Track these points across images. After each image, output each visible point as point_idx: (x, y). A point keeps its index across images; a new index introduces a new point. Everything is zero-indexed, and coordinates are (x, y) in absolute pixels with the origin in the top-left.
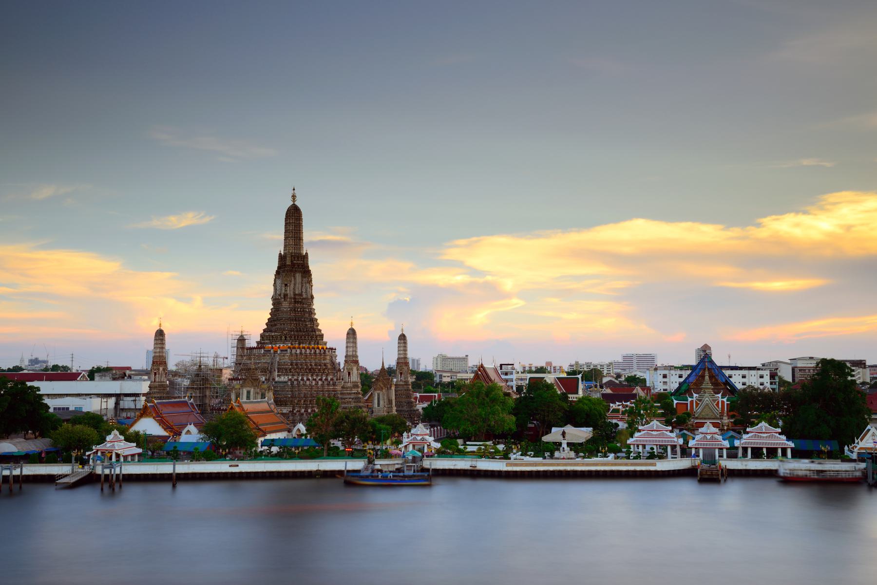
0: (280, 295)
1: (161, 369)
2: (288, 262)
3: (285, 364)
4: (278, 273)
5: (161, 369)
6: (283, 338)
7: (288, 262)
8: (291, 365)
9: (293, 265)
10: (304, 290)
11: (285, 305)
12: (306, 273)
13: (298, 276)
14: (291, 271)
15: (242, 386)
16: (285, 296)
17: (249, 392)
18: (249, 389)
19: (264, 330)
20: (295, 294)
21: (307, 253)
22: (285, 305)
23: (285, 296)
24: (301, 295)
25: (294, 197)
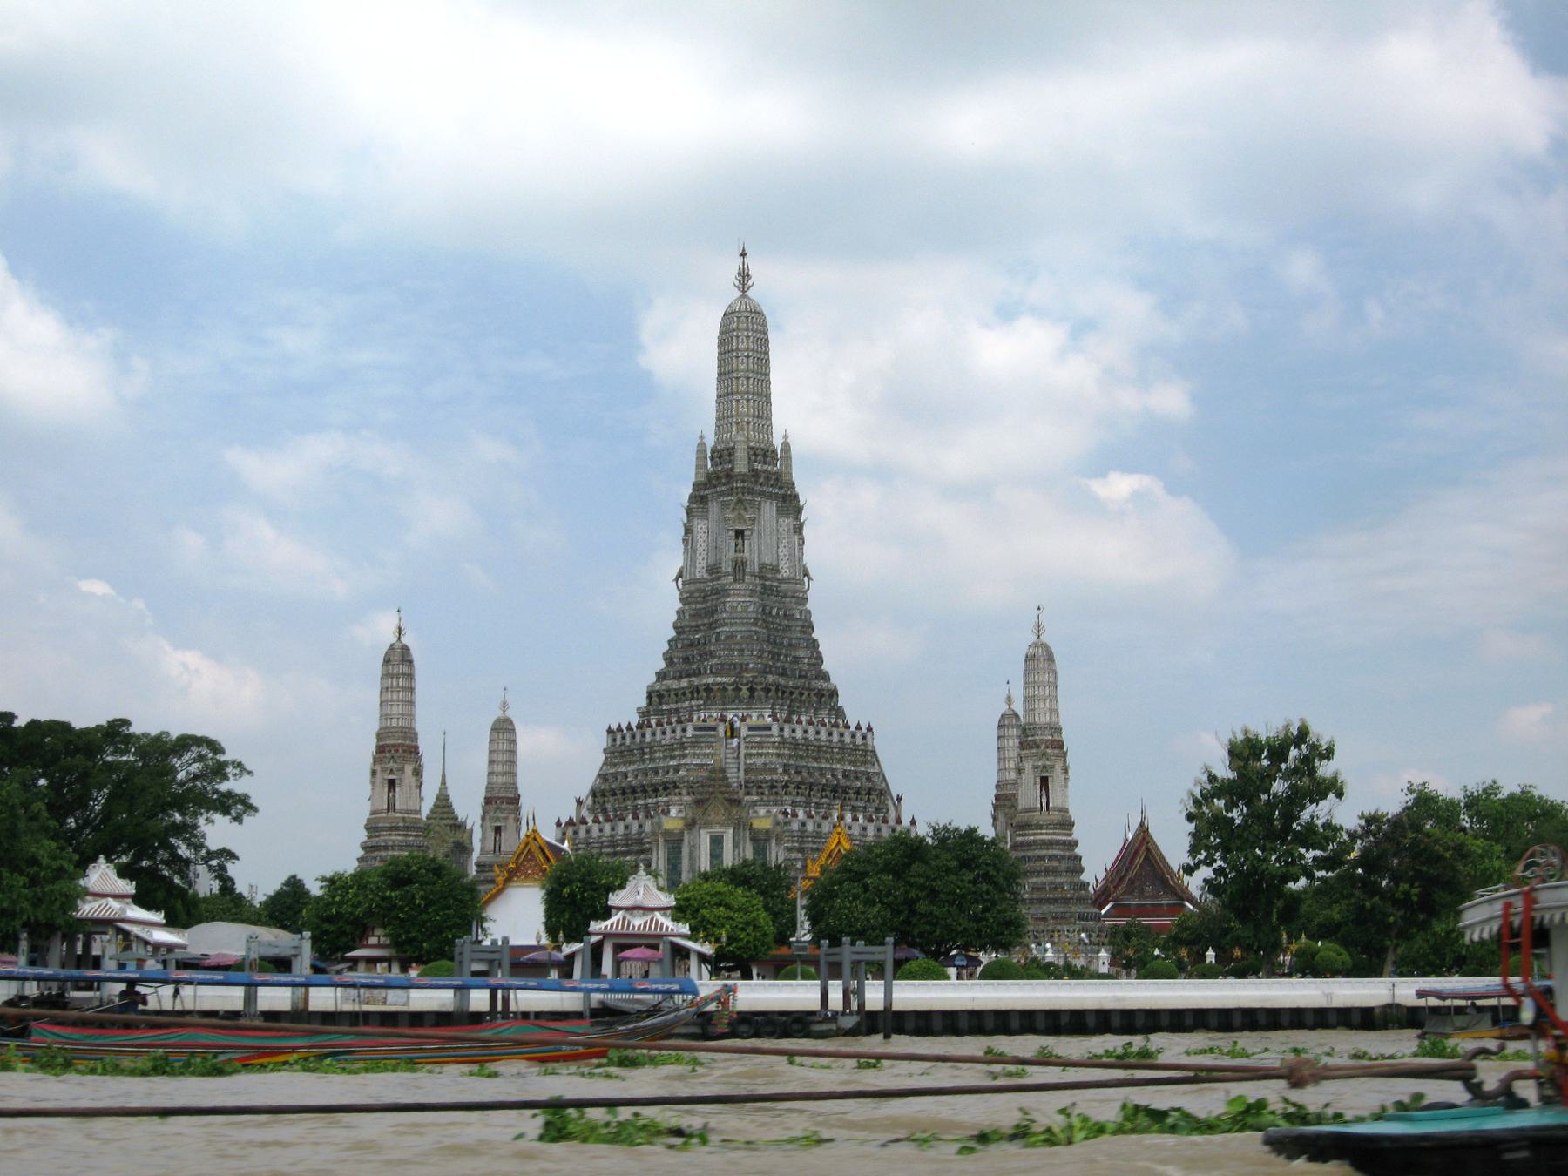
0: (714, 570)
1: (409, 769)
2: (741, 467)
3: (766, 769)
4: (699, 500)
5: (409, 769)
6: (745, 692)
7: (741, 467)
8: (786, 772)
9: (755, 474)
10: (784, 553)
11: (740, 600)
12: (790, 504)
13: (769, 509)
14: (751, 492)
15: (691, 825)
16: (739, 567)
18: (717, 829)
19: (661, 676)
20: (763, 566)
21: (786, 447)
22: (740, 600)
23: (739, 567)
24: (776, 570)
25: (744, 276)
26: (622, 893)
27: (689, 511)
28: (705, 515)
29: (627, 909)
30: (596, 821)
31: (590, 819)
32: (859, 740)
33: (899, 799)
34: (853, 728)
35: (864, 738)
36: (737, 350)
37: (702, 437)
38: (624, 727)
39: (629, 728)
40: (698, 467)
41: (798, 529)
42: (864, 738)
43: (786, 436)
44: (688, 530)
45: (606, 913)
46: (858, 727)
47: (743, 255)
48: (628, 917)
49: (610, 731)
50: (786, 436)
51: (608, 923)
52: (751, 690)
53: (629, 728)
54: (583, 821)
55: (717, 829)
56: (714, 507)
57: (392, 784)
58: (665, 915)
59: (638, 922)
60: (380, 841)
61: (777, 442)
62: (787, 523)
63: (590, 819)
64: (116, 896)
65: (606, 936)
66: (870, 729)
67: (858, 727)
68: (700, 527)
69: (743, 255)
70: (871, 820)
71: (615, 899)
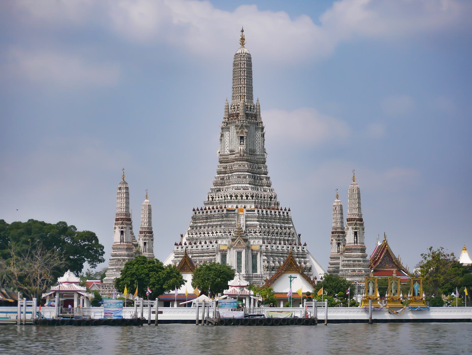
17: (239, 254)
26: (232, 281)
27: (222, 129)
28: (228, 129)
29: (235, 286)
30: (190, 244)
31: (187, 243)
32: (285, 214)
33: (299, 235)
34: (283, 210)
35: (287, 213)
36: (241, 68)
37: (227, 101)
38: (199, 209)
39: (202, 210)
40: (226, 112)
41: (263, 136)
42: (287, 213)
43: (258, 101)
44: (222, 135)
45: (227, 287)
46: (285, 210)
47: (242, 31)
49: (194, 210)
50: (258, 101)
52: (247, 196)
53: (202, 210)
54: (185, 244)
55: (240, 250)
56: (232, 128)
57: (122, 233)
58: (246, 288)
59: (238, 290)
60: (118, 253)
61: (255, 102)
62: (259, 133)
63: (187, 243)
64: (75, 283)
66: (289, 210)
67: (285, 210)
68: (226, 134)
69: (242, 31)
70: (291, 245)
71: (230, 283)
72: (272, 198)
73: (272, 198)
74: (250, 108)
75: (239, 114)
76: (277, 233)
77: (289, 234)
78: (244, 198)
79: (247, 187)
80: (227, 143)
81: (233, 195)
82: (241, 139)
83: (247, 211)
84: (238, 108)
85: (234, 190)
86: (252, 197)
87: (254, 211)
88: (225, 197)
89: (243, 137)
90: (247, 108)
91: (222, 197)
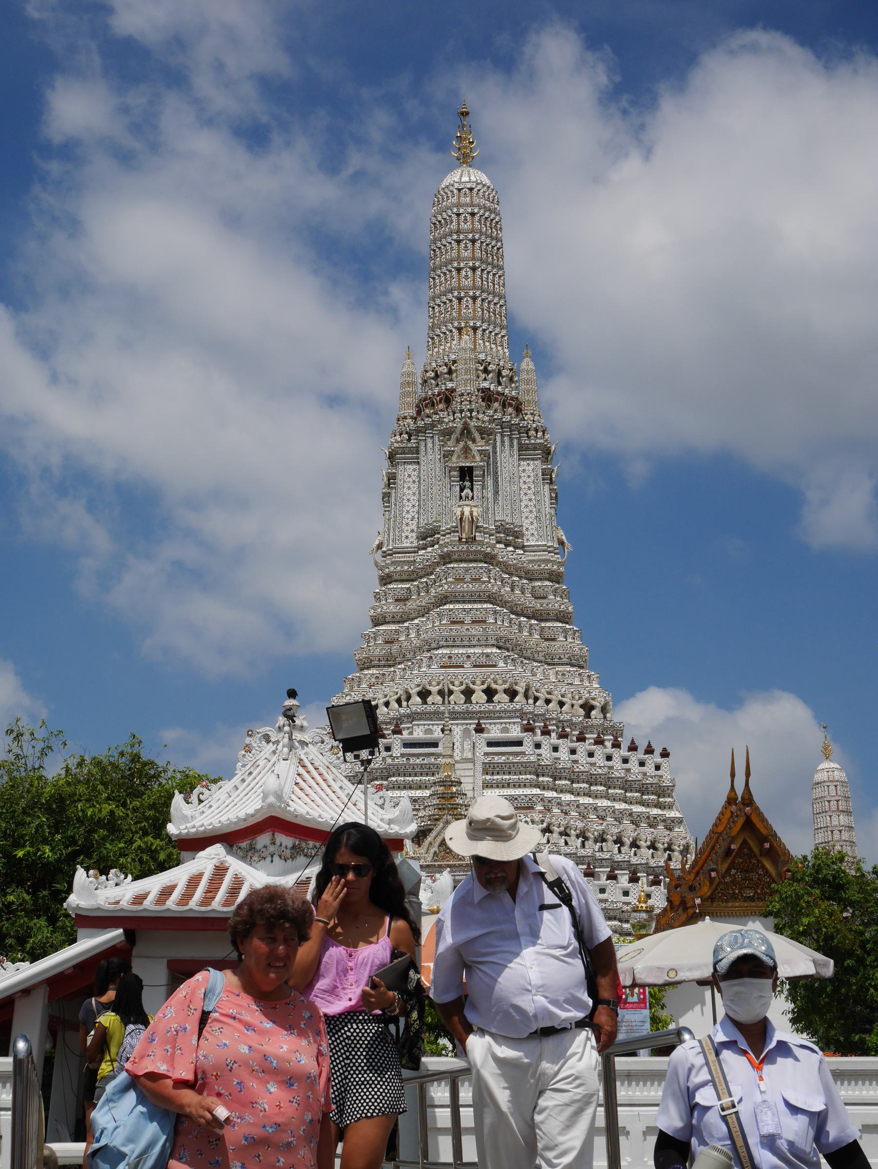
29: (235, 839)
44: (391, 479)
48: (236, 866)
51: (154, 884)
52: (490, 693)
65: (137, 927)
72: (592, 708)
73: (592, 708)
74: (499, 374)
75: (453, 390)
76: (619, 841)
77: (669, 848)
78: (479, 697)
79: (488, 655)
80: (408, 506)
81: (434, 689)
82: (462, 479)
83: (490, 744)
84: (450, 372)
85: (435, 669)
86: (512, 694)
87: (519, 743)
88: (399, 701)
89: (470, 470)
90: (486, 371)
91: (387, 704)
